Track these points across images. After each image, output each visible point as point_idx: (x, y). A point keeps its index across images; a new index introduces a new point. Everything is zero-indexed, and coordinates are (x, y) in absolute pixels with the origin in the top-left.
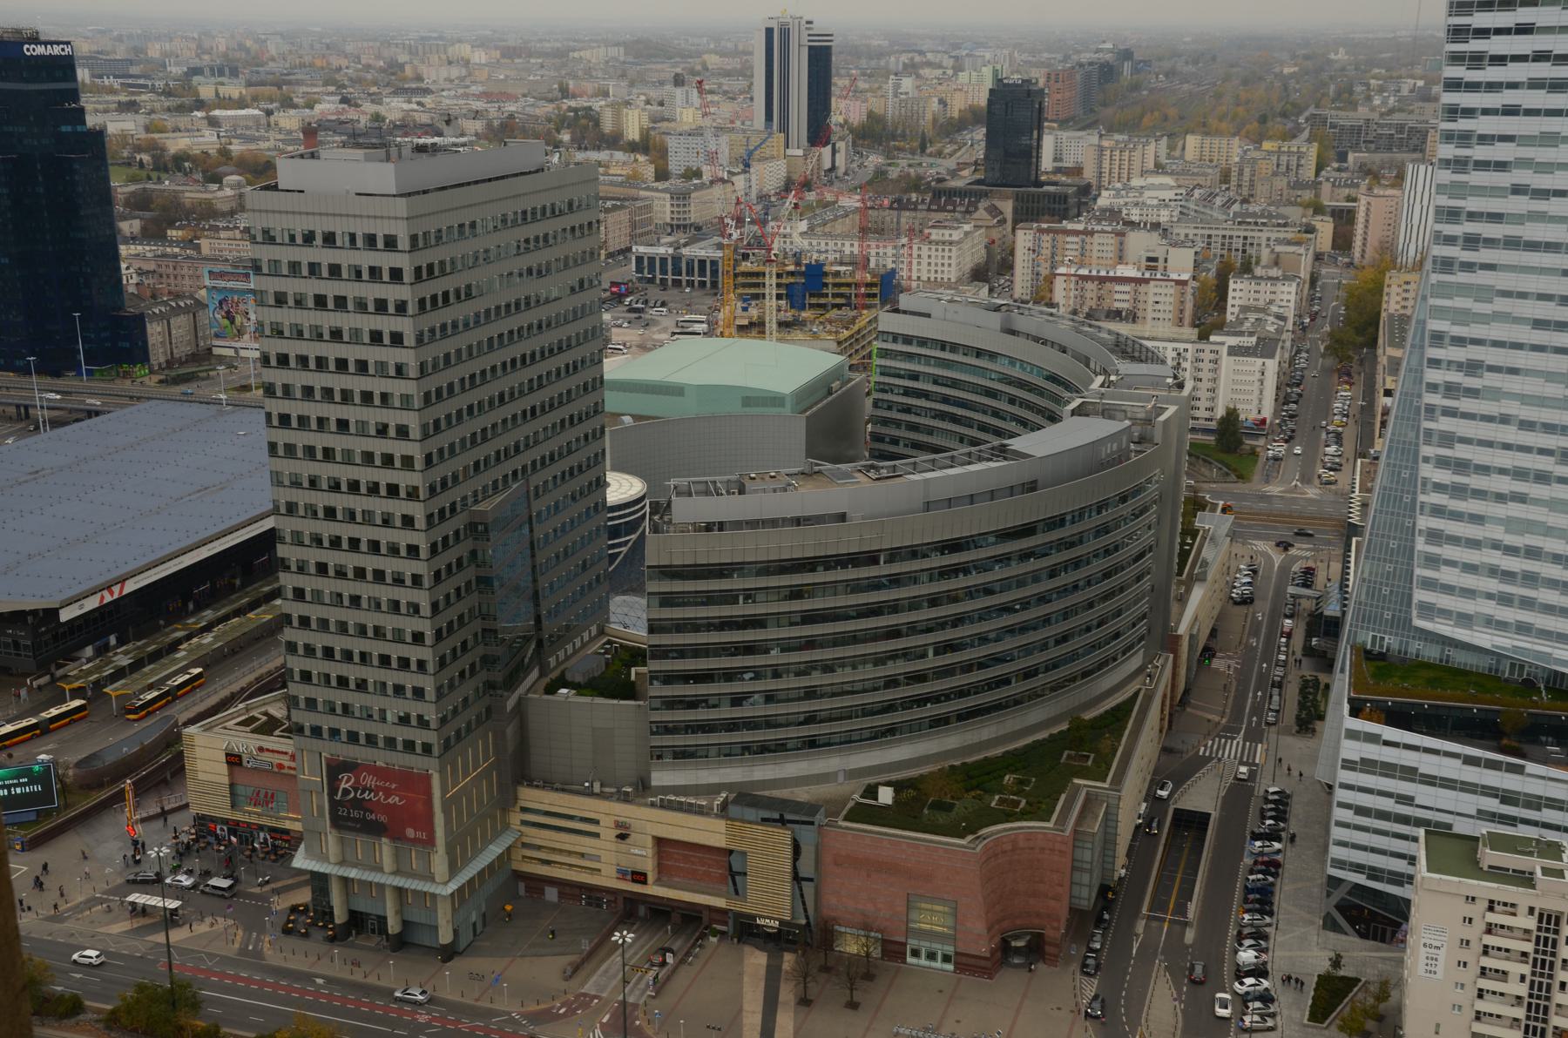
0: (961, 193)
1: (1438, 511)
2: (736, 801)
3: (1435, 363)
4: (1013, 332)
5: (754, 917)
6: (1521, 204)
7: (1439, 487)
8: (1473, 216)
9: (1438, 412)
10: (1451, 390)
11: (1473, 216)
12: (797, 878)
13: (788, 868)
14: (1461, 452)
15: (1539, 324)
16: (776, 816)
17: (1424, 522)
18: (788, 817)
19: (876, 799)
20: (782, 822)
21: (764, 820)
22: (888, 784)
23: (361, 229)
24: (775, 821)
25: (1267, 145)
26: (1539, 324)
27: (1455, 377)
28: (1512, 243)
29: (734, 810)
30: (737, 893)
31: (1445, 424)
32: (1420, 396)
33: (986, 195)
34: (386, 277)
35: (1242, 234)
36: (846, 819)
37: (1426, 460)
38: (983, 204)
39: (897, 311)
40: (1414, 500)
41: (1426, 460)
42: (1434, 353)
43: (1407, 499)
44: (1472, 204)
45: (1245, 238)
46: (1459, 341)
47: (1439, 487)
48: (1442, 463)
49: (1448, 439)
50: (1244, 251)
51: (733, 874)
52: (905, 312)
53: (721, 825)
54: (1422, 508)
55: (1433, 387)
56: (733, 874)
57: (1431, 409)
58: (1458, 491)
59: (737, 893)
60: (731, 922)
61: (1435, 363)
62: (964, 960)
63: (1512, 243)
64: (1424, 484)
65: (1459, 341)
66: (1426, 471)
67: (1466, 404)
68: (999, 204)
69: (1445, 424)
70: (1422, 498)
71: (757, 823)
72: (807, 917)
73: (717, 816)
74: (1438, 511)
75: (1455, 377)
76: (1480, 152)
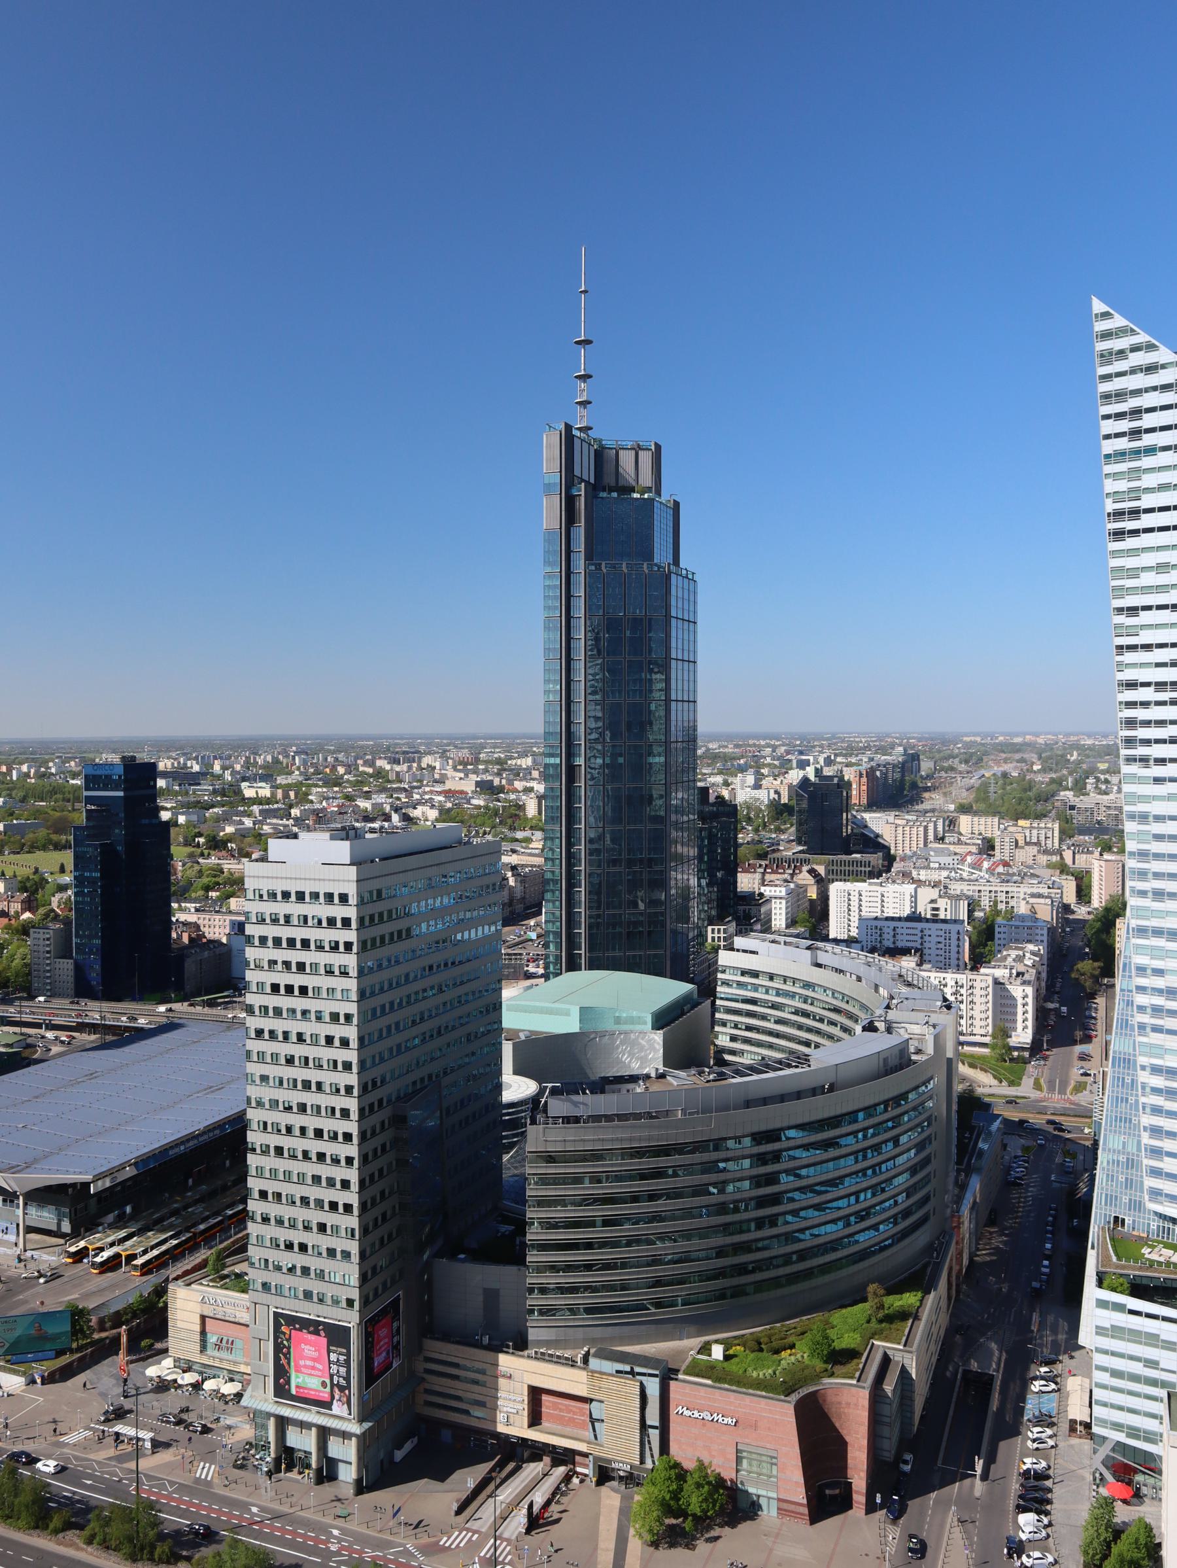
0: (790, 862)
1: (1157, 1110)
2: (596, 1356)
3: (1141, 989)
4: (819, 966)
5: (609, 1461)
7: (1156, 1091)
8: (1158, 875)
9: (1148, 1030)
11: (1158, 875)
12: (644, 1426)
13: (637, 1417)
16: (627, 1368)
17: (1147, 1120)
18: (637, 1369)
19: (710, 1355)
20: (632, 1373)
21: (618, 1372)
22: (717, 1342)
23: (322, 889)
24: (626, 1373)
25: (1021, 823)
27: (1159, 1001)
29: (594, 1363)
30: (596, 1438)
31: (1156, 1038)
32: (1132, 1016)
33: (807, 861)
34: (339, 924)
35: (1005, 889)
36: (686, 1373)
37: (1143, 1068)
38: (805, 868)
39: (732, 949)
40: (1137, 1101)
41: (1143, 1068)
42: (1142, 981)
43: (1132, 1100)
45: (1007, 892)
47: (1156, 1091)
48: (1156, 1070)
50: (1007, 903)
51: (593, 1421)
52: (738, 950)
53: (582, 1375)
54: (1144, 1108)
55: (1141, 1009)
56: (593, 1421)
57: (1142, 1027)
59: (596, 1438)
60: (591, 1466)
61: (1141, 989)
62: (785, 1506)
64: (1143, 1088)
66: (1144, 1077)
68: (816, 867)
70: (1143, 1100)
71: (612, 1375)
72: (654, 1462)
73: (579, 1368)
74: (1157, 1110)
75: (1159, 1001)
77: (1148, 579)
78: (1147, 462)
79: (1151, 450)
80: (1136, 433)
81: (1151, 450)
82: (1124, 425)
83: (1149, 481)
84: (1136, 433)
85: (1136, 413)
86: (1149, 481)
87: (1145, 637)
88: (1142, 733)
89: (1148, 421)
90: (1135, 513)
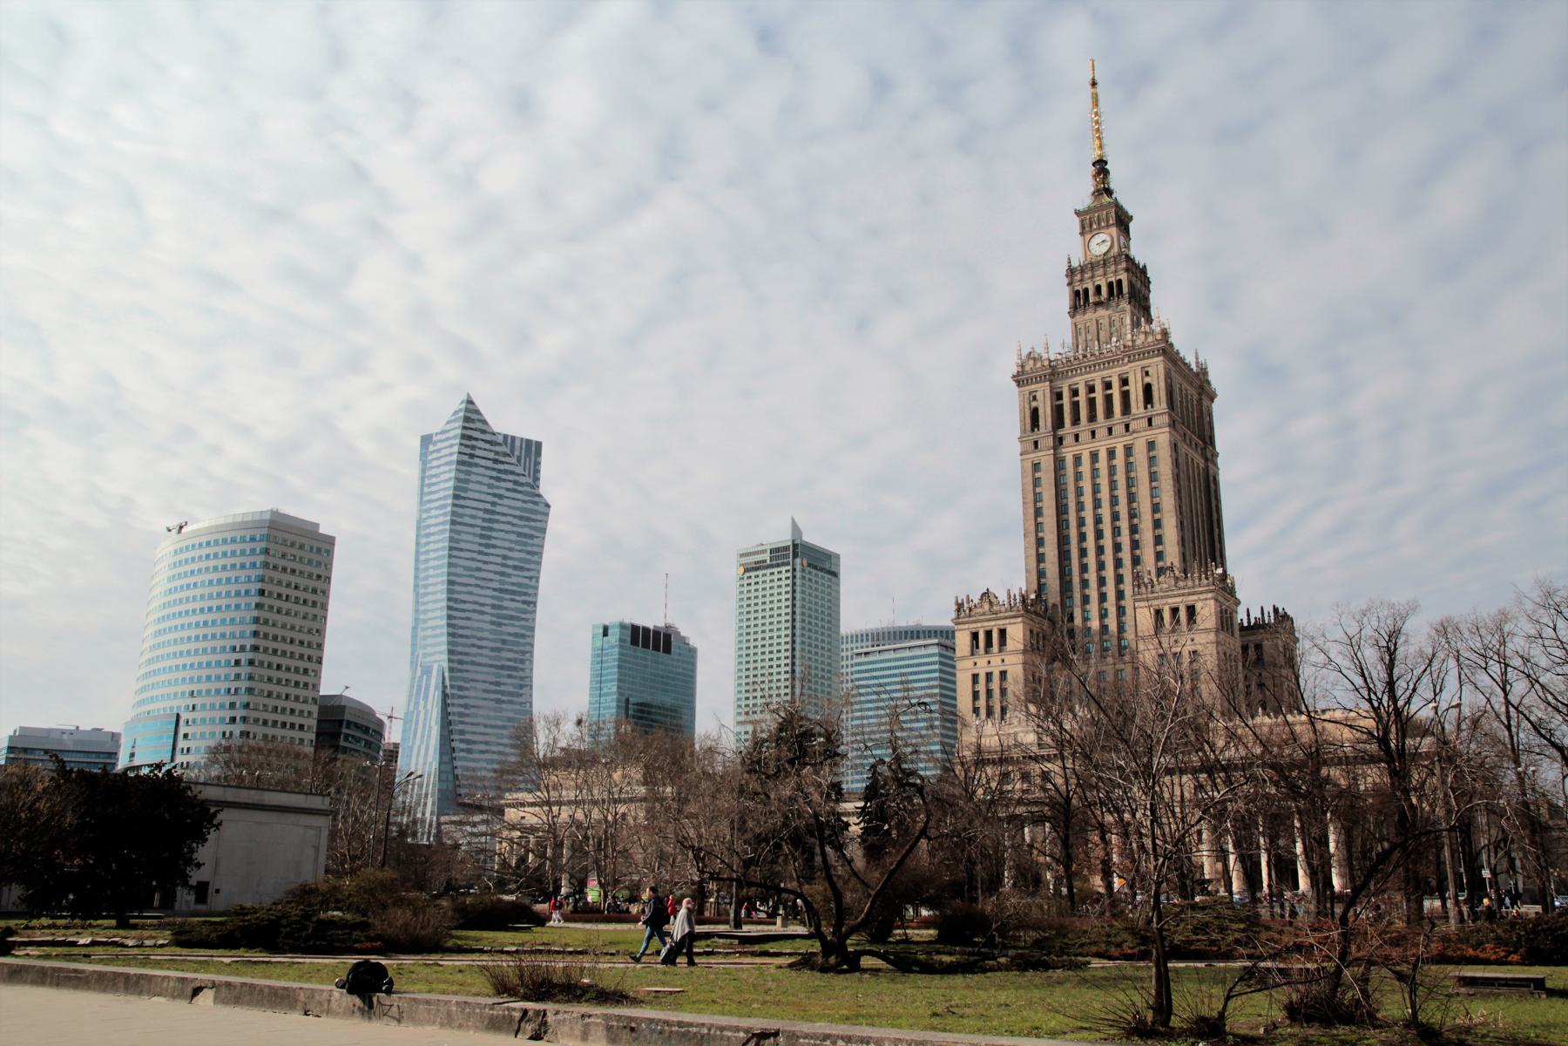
6: (475, 650)
10: (461, 715)
14: (468, 737)
15: (485, 691)
26: (485, 691)
28: (473, 663)
31: (461, 727)
44: (460, 649)
46: (460, 697)
48: (462, 741)
49: (462, 732)
58: (469, 751)
63: (473, 663)
65: (460, 697)
67: (466, 719)
69: (461, 727)
76: (460, 632)
77: (466, 520)
78: (474, 470)
79: (476, 465)
80: (472, 456)
81: (476, 465)
82: (468, 451)
83: (473, 478)
84: (472, 456)
85: (473, 447)
86: (473, 478)
87: (462, 545)
88: (457, 588)
89: (478, 452)
90: (466, 490)
